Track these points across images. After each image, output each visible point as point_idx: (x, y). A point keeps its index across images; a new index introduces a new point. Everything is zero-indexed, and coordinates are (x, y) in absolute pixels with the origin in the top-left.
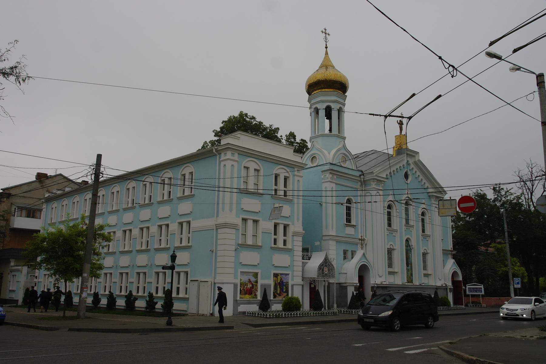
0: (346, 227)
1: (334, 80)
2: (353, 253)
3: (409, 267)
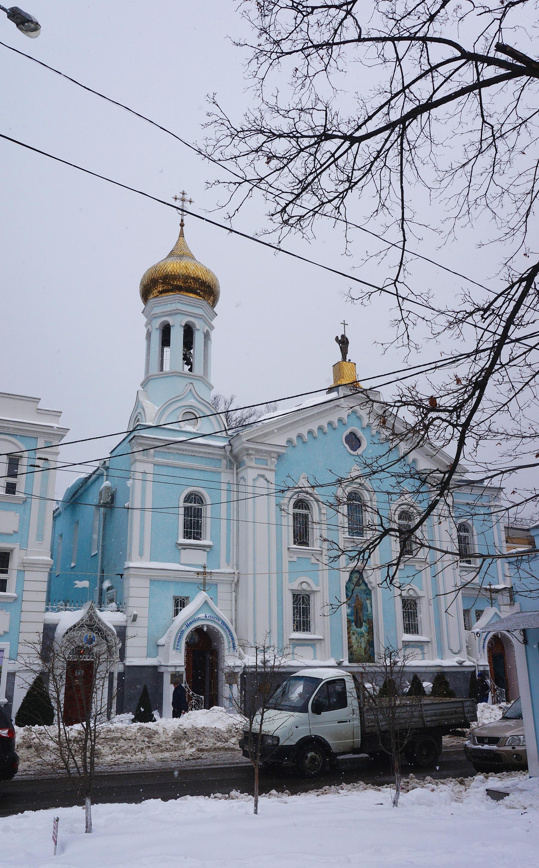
0: (182, 551)
1: (173, 273)
2: (479, 614)
3: (363, 629)
